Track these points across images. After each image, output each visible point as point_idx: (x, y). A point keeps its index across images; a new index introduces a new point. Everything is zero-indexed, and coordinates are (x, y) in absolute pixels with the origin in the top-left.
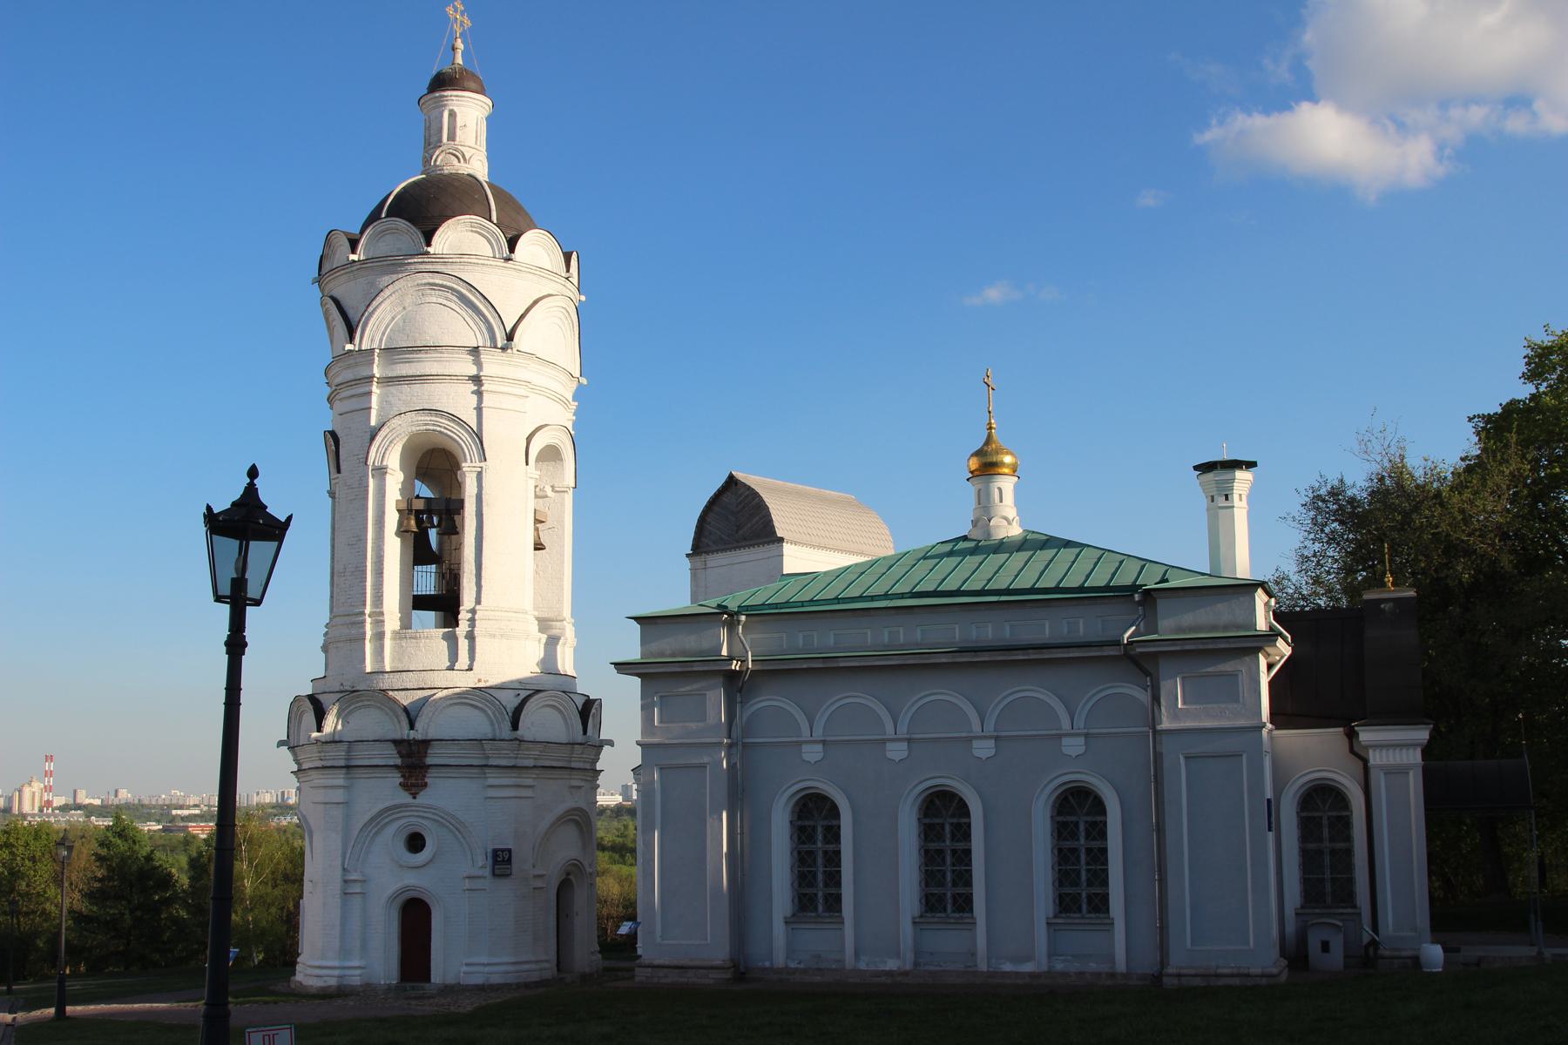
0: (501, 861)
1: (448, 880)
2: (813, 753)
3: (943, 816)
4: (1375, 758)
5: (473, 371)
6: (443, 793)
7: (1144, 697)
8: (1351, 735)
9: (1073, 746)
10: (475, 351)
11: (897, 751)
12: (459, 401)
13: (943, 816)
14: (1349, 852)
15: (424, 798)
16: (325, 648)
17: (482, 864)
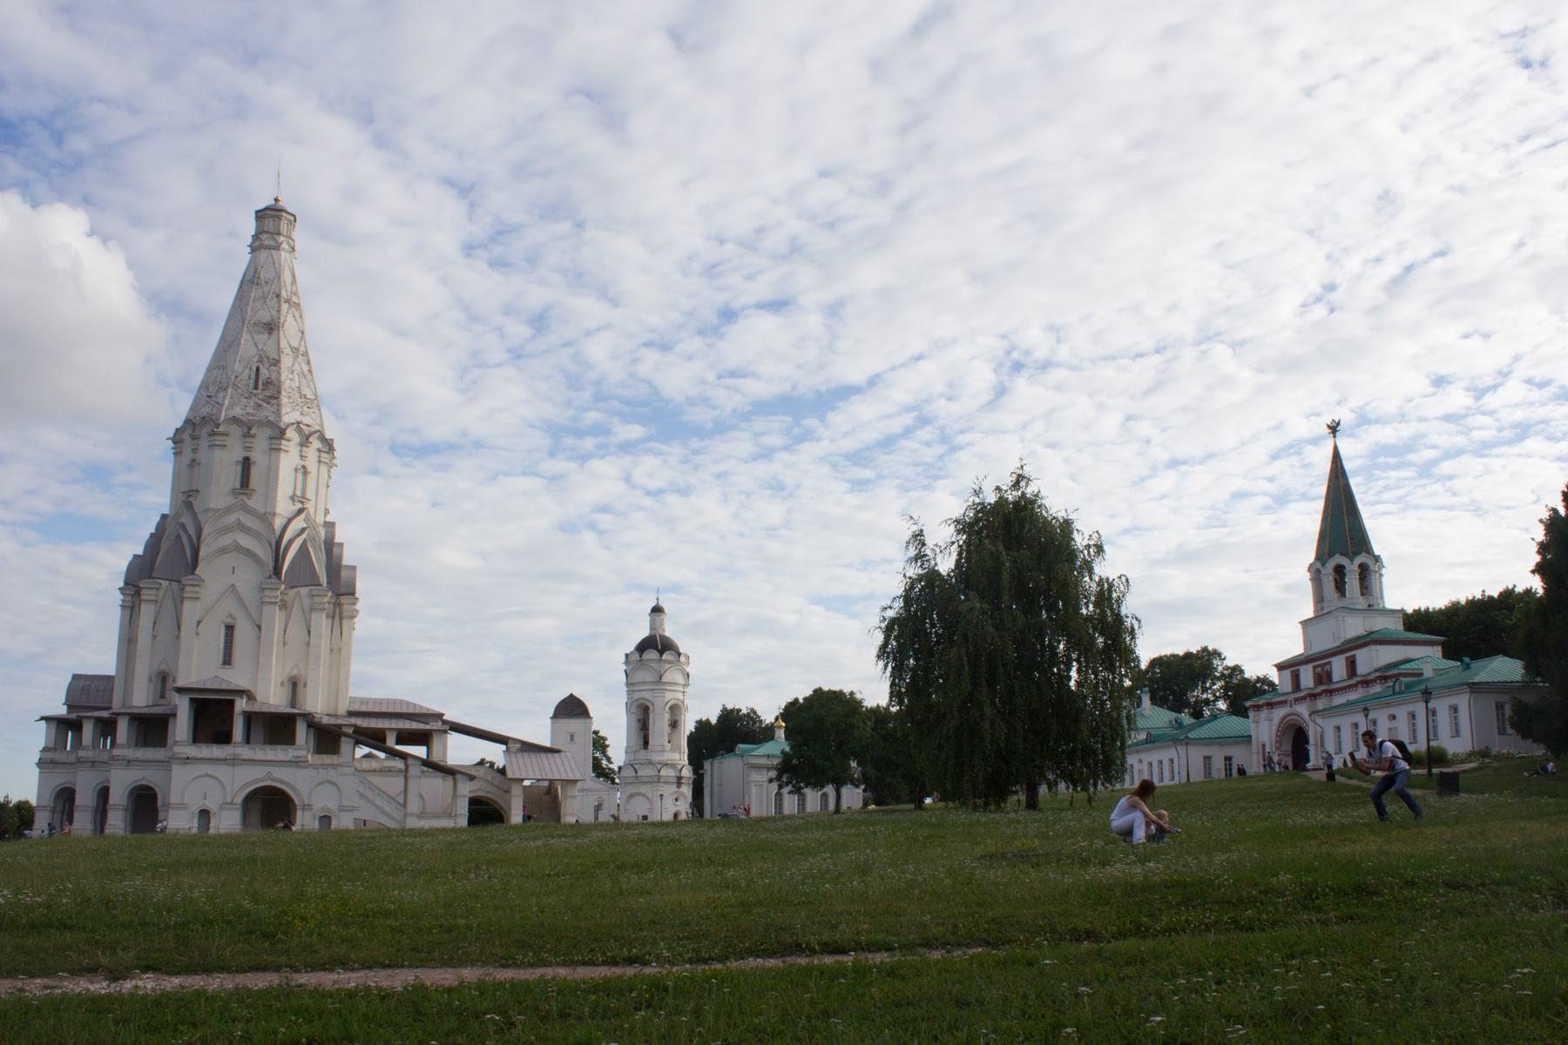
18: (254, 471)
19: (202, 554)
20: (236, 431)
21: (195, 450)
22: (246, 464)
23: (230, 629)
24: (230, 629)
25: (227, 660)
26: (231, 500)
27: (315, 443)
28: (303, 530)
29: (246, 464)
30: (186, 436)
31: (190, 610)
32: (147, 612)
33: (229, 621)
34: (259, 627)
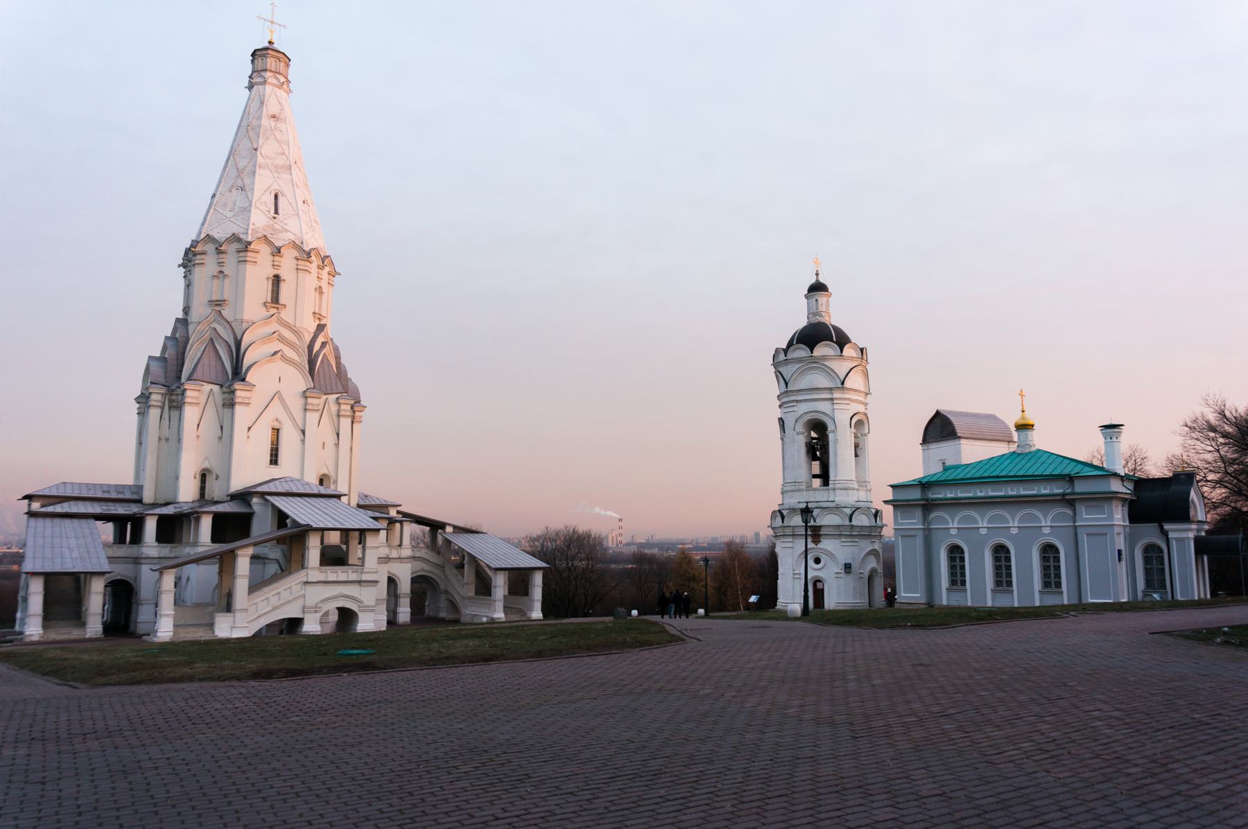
0: (848, 567)
1: (829, 573)
2: (954, 532)
3: (1001, 553)
4: (1171, 535)
5: (829, 396)
6: (826, 544)
7: (1071, 513)
8: (1161, 527)
9: (1046, 531)
10: (830, 389)
11: (983, 532)
12: (824, 407)
13: (1001, 553)
14: (1163, 569)
15: (820, 546)
16: (782, 493)
17: (839, 569)
18: (283, 286)
19: (247, 361)
20: (265, 250)
21: (220, 264)
22: (277, 280)
23: (276, 431)
24: (276, 431)
25: (274, 460)
26: (263, 313)
27: (327, 269)
28: (324, 344)
29: (277, 280)
30: (210, 248)
31: (242, 415)
32: (190, 414)
33: (277, 425)
34: (303, 432)
